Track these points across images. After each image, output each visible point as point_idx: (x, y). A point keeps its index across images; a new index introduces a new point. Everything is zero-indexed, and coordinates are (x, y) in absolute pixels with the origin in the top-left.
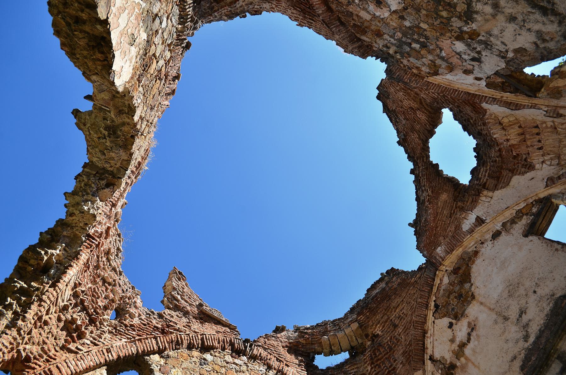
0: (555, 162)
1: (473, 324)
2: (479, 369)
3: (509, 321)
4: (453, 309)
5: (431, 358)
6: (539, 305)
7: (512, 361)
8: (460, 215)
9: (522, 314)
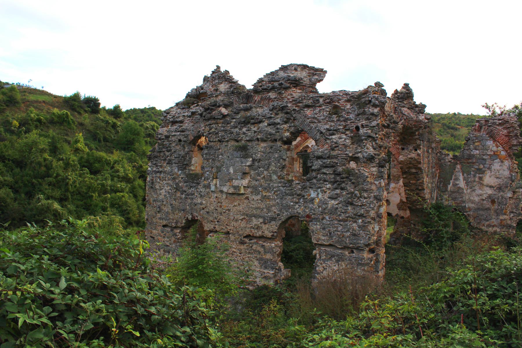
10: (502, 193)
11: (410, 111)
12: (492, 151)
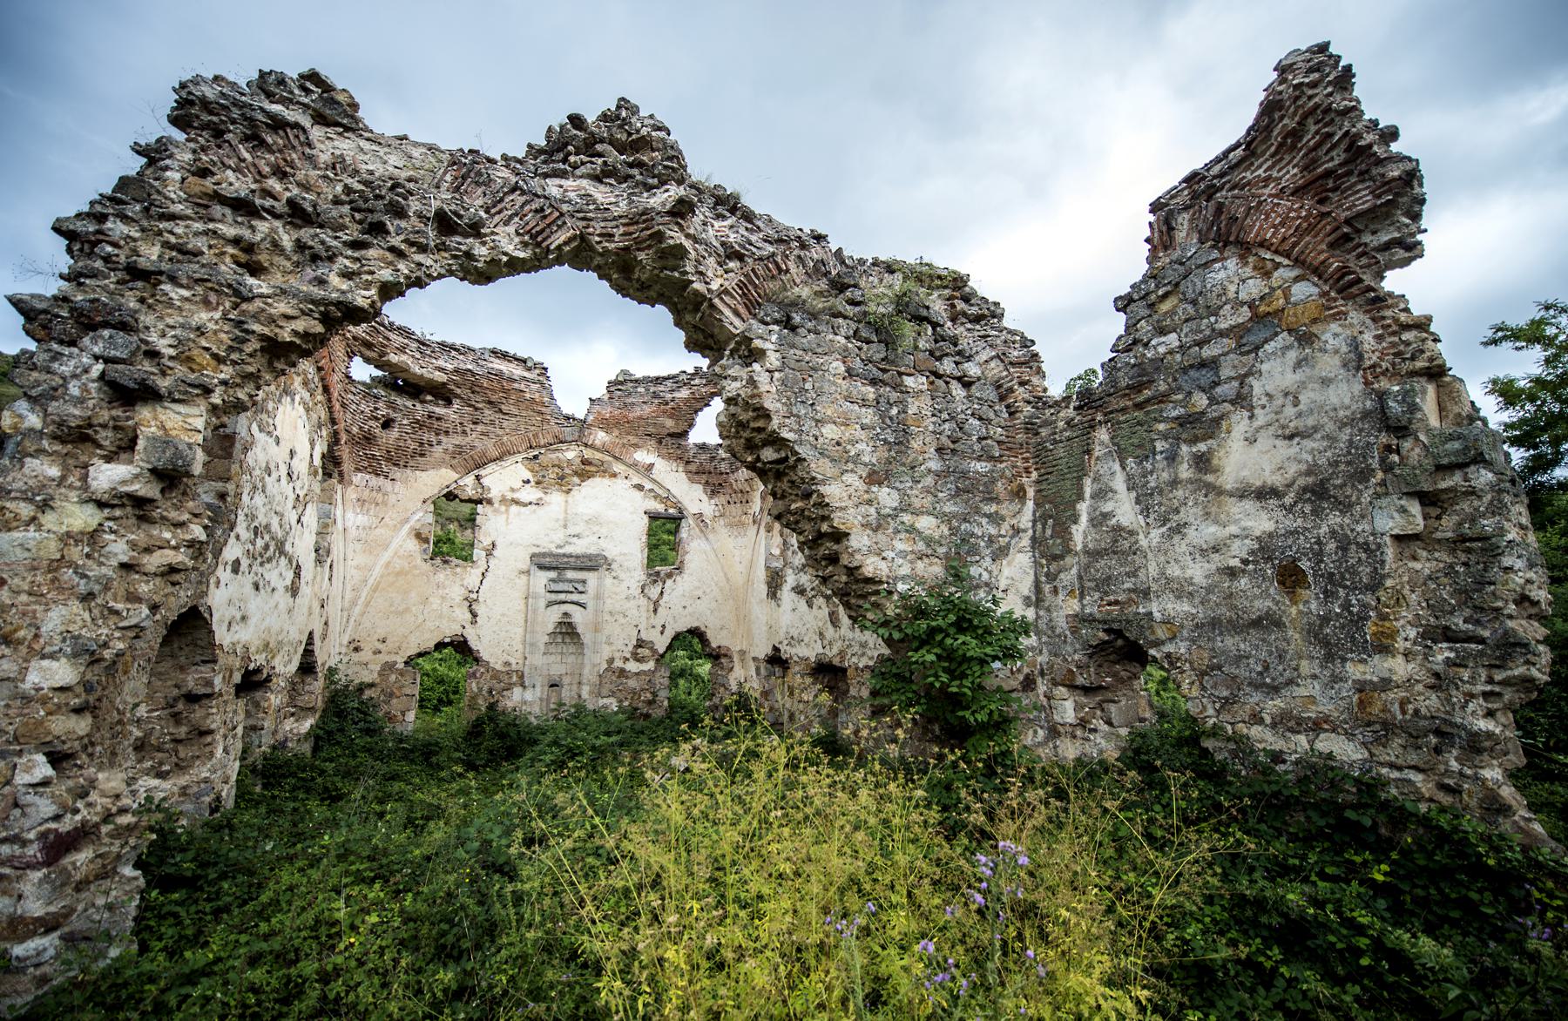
0: (717, 514)
4: (544, 476)
10: (1335, 519)
11: (608, 189)
12: (1243, 304)
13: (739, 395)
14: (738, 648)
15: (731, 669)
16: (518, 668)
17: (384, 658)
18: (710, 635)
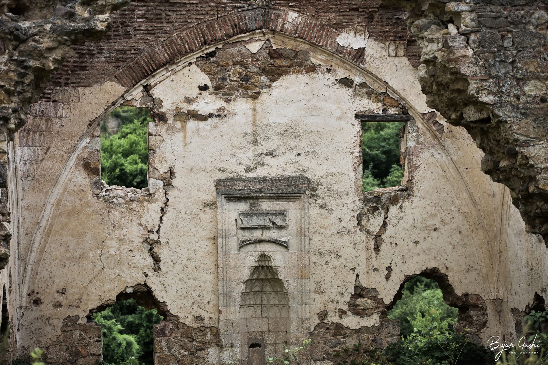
1: (225, 113)
2: (186, 145)
3: (255, 147)
5: (147, 89)
6: (288, 165)
7: (219, 170)
8: (358, 23)
9: (270, 155)
13: (435, 58)
14: (493, 296)
15: (484, 324)
16: (212, 323)
17: (65, 312)
18: (453, 279)
